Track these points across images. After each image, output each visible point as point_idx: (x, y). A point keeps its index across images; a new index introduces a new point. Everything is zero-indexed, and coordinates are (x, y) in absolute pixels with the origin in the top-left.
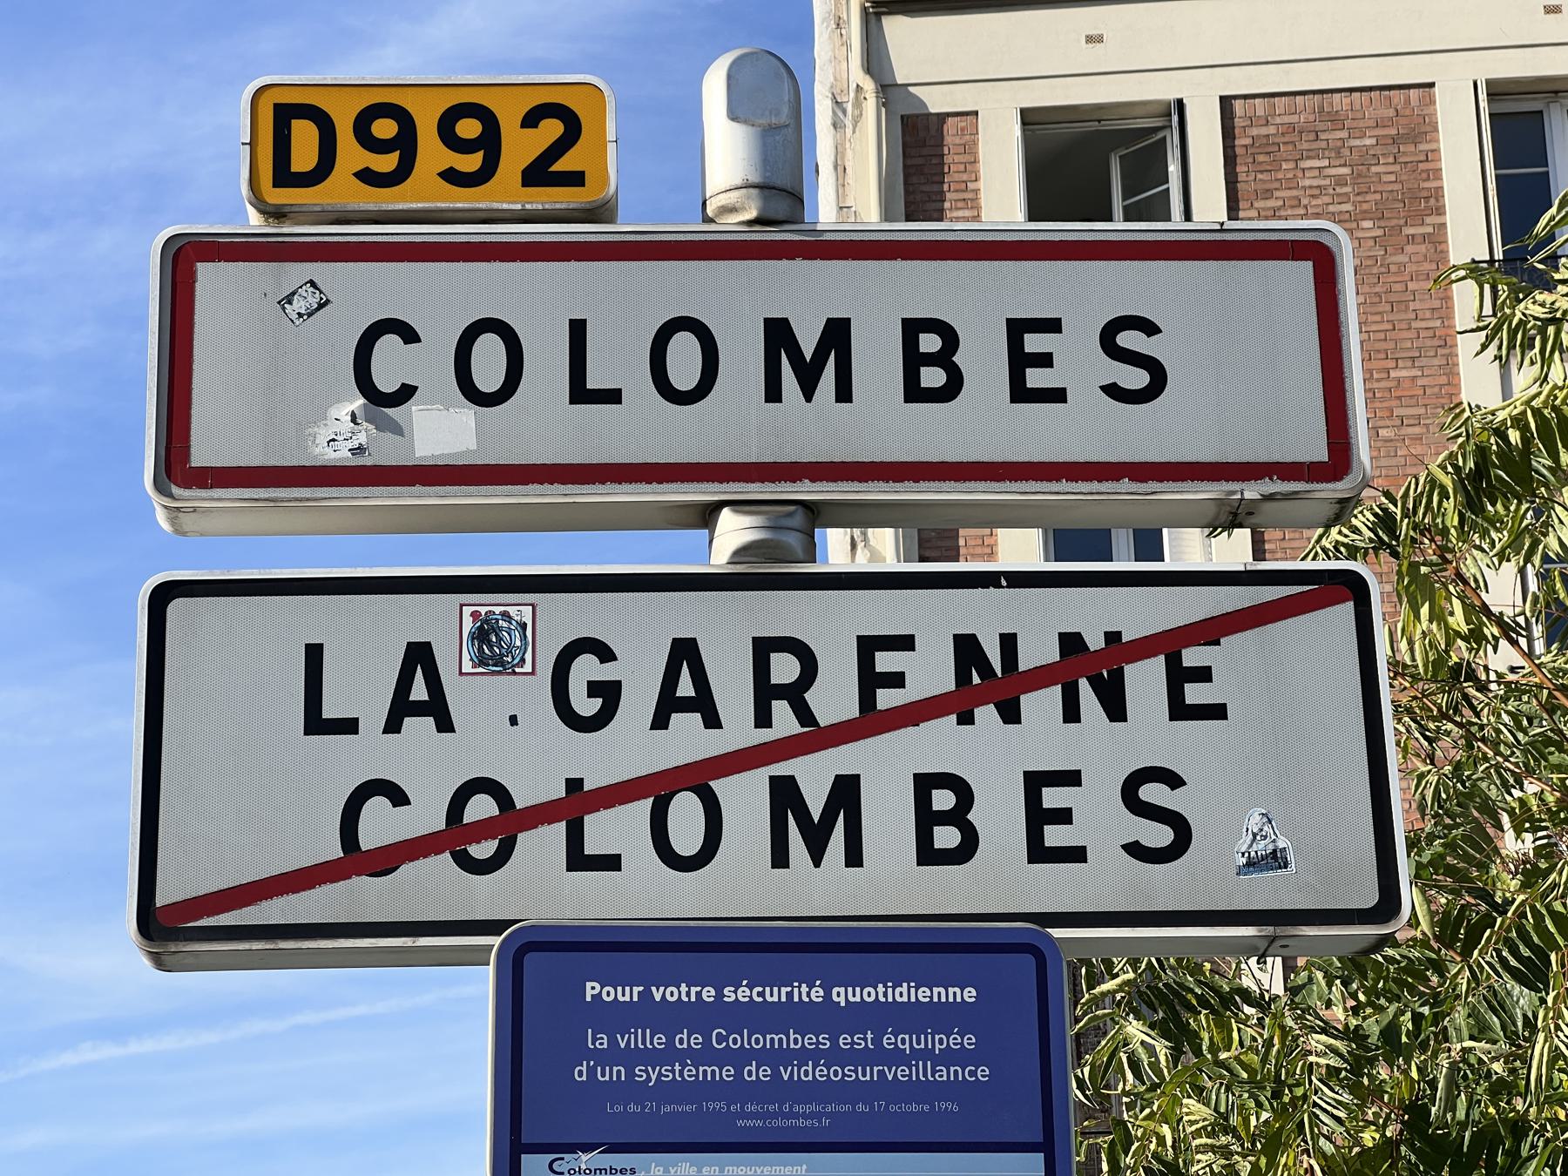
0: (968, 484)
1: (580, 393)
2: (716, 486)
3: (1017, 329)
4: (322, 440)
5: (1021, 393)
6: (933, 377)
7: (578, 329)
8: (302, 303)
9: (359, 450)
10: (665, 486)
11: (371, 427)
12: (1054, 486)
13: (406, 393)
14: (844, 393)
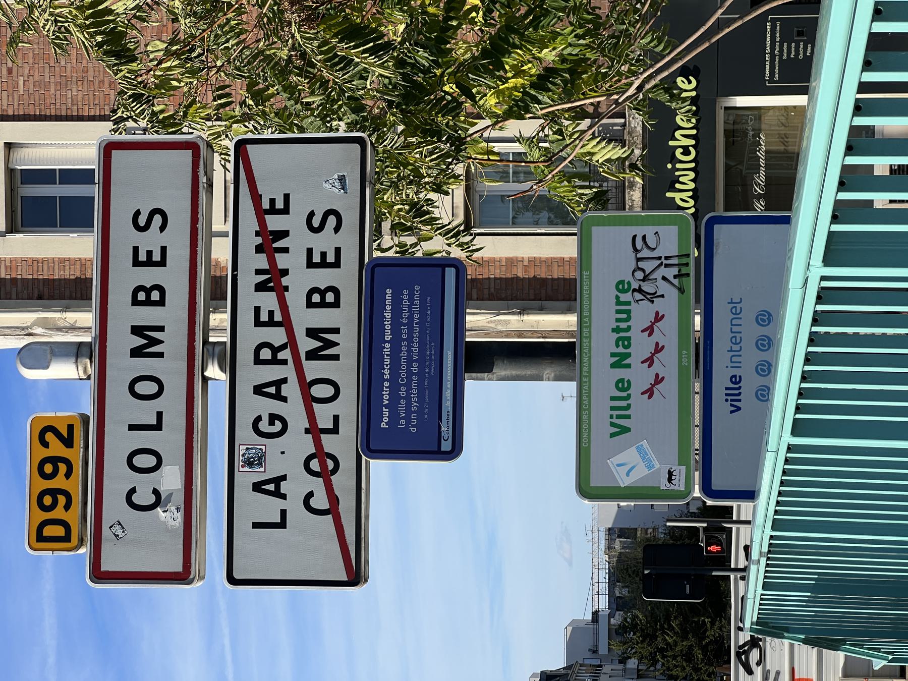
0: (198, 284)
1: (158, 427)
2: (196, 377)
3: (136, 263)
4: (173, 523)
5: (162, 263)
6: (155, 295)
7: (132, 427)
8: (118, 531)
9: (178, 509)
10: (195, 396)
11: (169, 505)
12: (199, 253)
13: (156, 492)
14: (161, 329)
